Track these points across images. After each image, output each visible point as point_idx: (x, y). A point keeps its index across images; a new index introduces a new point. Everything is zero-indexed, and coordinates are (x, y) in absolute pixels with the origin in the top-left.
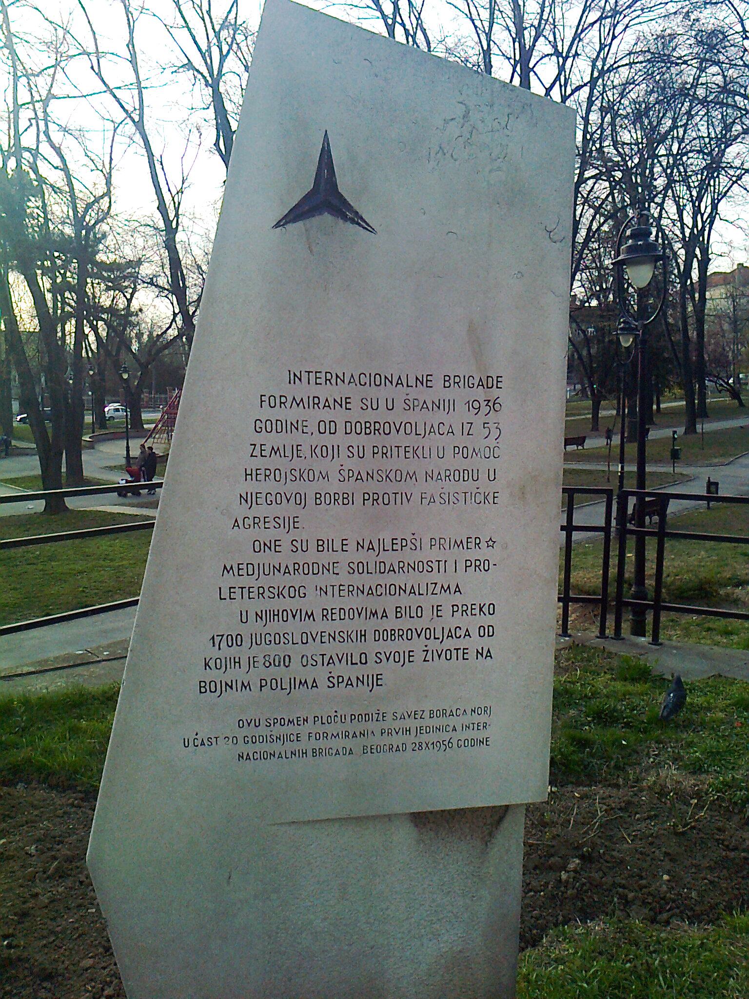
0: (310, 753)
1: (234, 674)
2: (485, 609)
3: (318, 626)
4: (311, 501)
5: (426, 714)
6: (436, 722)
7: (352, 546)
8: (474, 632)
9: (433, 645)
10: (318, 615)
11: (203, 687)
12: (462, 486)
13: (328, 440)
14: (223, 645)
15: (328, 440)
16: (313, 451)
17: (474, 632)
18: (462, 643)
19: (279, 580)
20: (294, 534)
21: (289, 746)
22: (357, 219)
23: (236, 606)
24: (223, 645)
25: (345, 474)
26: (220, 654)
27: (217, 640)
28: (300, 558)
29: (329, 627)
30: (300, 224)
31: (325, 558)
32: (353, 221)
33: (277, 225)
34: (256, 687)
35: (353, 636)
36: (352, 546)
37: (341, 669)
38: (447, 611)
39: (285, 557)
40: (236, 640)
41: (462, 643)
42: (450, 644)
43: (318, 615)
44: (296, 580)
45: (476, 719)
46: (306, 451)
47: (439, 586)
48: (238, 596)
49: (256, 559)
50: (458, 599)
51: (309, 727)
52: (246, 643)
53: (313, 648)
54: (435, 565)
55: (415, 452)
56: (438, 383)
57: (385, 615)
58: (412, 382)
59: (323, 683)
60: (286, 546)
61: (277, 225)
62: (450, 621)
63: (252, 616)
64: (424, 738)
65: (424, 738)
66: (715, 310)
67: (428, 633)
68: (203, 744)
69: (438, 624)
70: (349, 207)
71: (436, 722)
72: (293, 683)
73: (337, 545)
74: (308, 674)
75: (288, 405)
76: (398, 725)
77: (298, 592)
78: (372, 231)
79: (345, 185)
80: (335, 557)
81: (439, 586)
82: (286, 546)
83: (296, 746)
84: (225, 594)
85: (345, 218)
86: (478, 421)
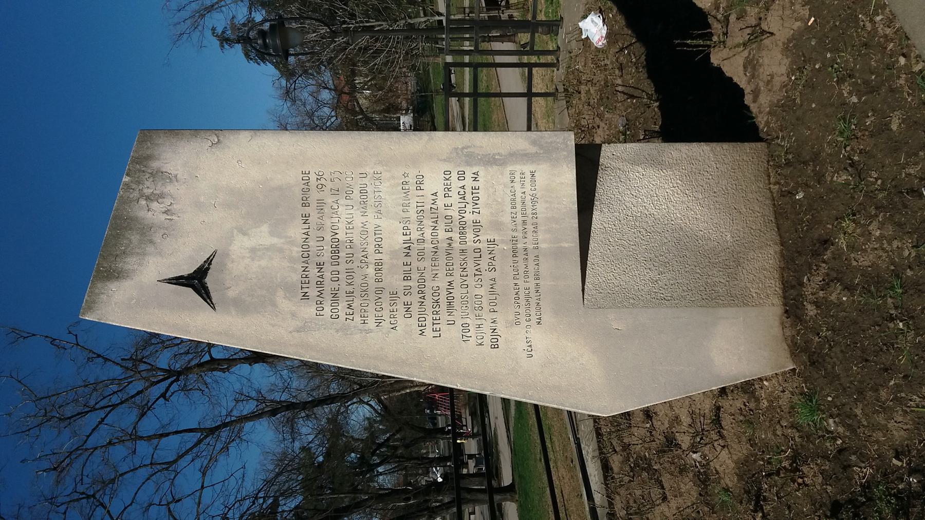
0: (537, 282)
1: (487, 328)
2: (447, 177)
3: (457, 280)
4: (380, 285)
5: (514, 211)
6: (519, 206)
7: (408, 260)
8: (462, 183)
9: (469, 208)
10: (450, 279)
11: (495, 346)
12: (371, 195)
13: (342, 276)
14: (468, 334)
15: (342, 276)
16: (350, 284)
17: (462, 183)
18: (468, 190)
19: (429, 302)
20: (400, 294)
21: (533, 294)
22: (209, 261)
23: (444, 327)
24: (468, 334)
25: (363, 265)
26: (474, 338)
27: (465, 338)
28: (415, 291)
29: (457, 273)
30: (212, 294)
31: (415, 276)
32: (210, 264)
33: (214, 308)
34: (494, 315)
35: (463, 257)
36: (408, 260)
37: (484, 265)
38: (448, 201)
39: (415, 299)
40: (465, 326)
41: (468, 190)
42: (469, 197)
43: (450, 279)
44: (428, 292)
45: (517, 179)
46: (350, 289)
47: (433, 206)
48: (438, 327)
49: (416, 316)
50: (441, 194)
51: (520, 283)
52: (468, 321)
53: (471, 281)
54: (420, 208)
55: (349, 223)
56: (307, 210)
57: (450, 239)
58: (306, 226)
59: (492, 275)
60: (407, 299)
61: (214, 308)
62: (455, 198)
63: (450, 318)
64: (529, 212)
65: (529, 212)
66: (233, 26)
67: (461, 211)
68: (530, 346)
69: (456, 207)
70: (202, 266)
71: (519, 206)
72: (492, 293)
73: (407, 268)
74: (487, 283)
75: (321, 299)
76: (520, 228)
77: (436, 291)
78: (215, 252)
79: (187, 269)
80: (414, 270)
81: (433, 206)
82: (407, 299)
83: (533, 290)
84: (437, 334)
85: (208, 269)
86: (330, 185)
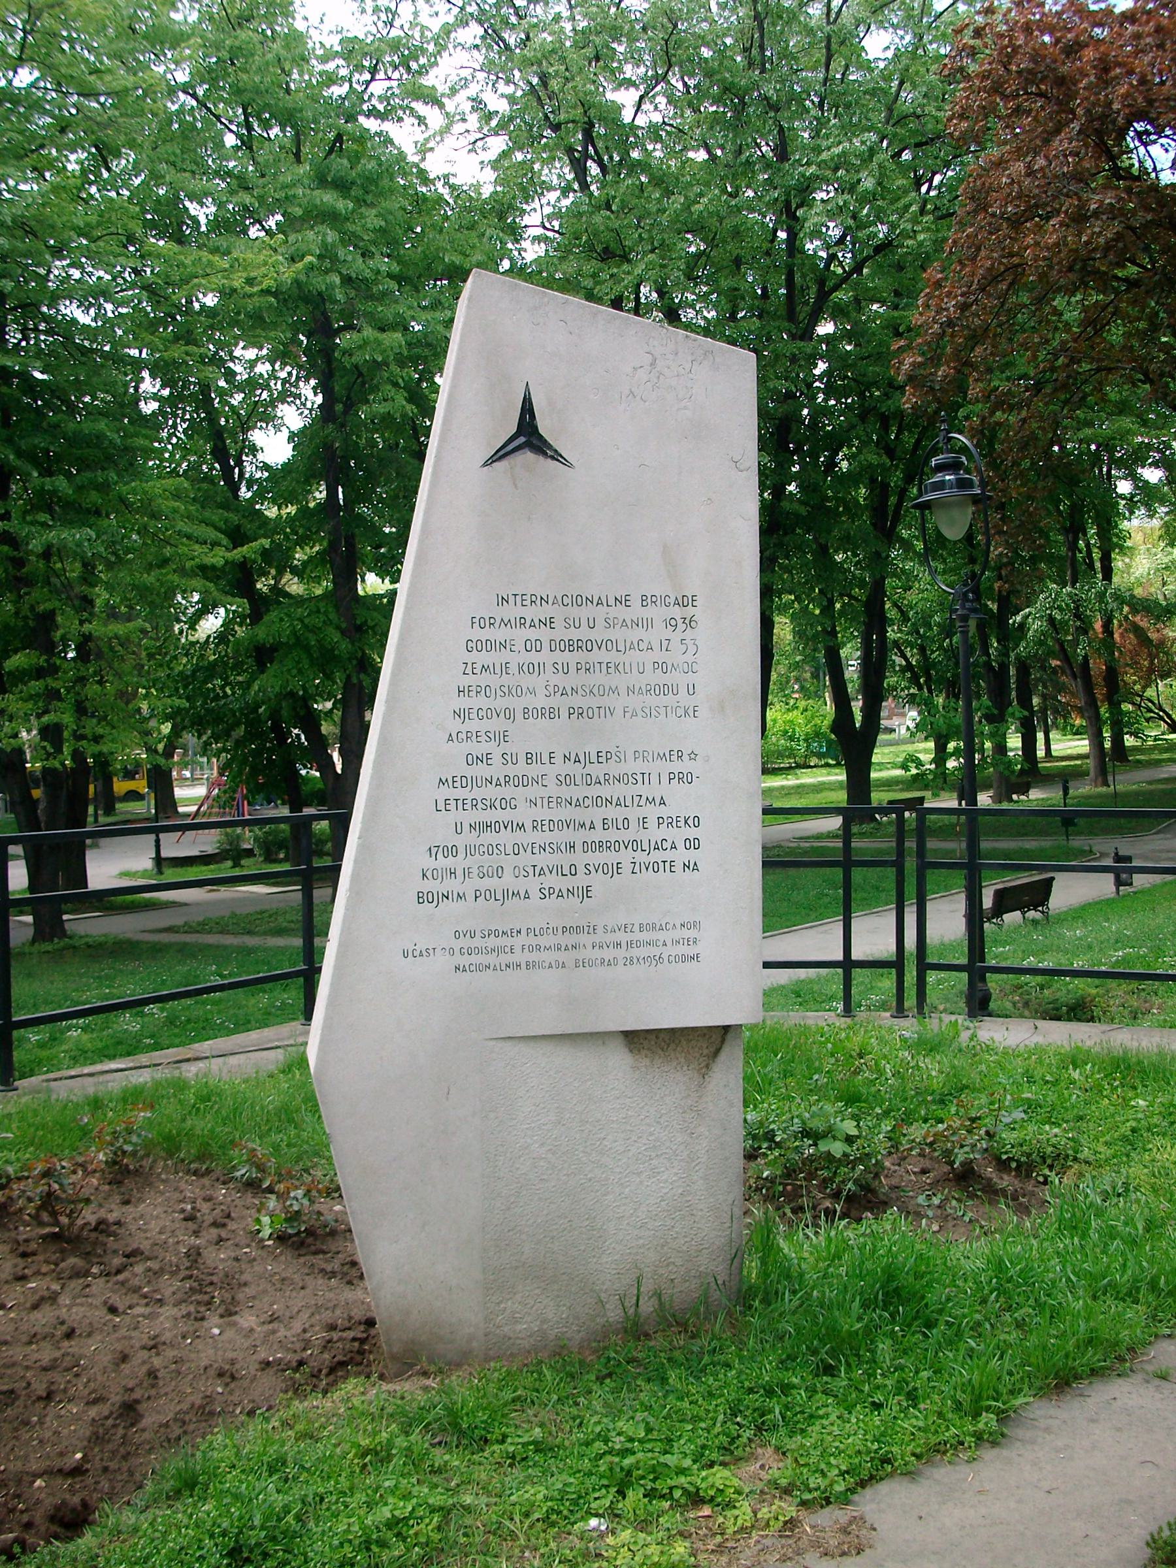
0: (523, 966)
1: (452, 885)
2: (690, 822)
4: (519, 715)
6: (645, 936)
7: (559, 759)
8: (680, 845)
9: (641, 857)
10: (528, 826)
13: (534, 657)
15: (534, 657)
16: (520, 668)
17: (680, 845)
18: (669, 855)
19: (491, 792)
21: (505, 959)
22: (557, 456)
23: (455, 815)
25: (551, 689)
27: (434, 850)
28: (511, 770)
29: (539, 838)
31: (534, 770)
32: (553, 458)
33: (485, 465)
34: (470, 896)
36: (559, 759)
37: (551, 880)
38: (652, 823)
39: (496, 770)
40: (452, 851)
41: (669, 855)
42: (657, 856)
43: (528, 826)
44: (507, 792)
45: (686, 933)
46: (513, 668)
48: (452, 807)
49: (470, 772)
50: (663, 811)
52: (461, 855)
53: (525, 859)
55: (616, 667)
56: (636, 602)
57: (592, 827)
58: (612, 601)
59: (535, 894)
60: (496, 759)
61: (485, 465)
62: (656, 833)
63: (466, 827)
65: (635, 952)
67: (635, 845)
69: (643, 836)
70: (550, 447)
71: (645, 936)
72: (506, 894)
73: (545, 759)
74: (521, 885)
77: (507, 804)
78: (571, 466)
79: (544, 426)
82: (496, 759)
84: (441, 806)
85: (545, 454)
86: (676, 637)
